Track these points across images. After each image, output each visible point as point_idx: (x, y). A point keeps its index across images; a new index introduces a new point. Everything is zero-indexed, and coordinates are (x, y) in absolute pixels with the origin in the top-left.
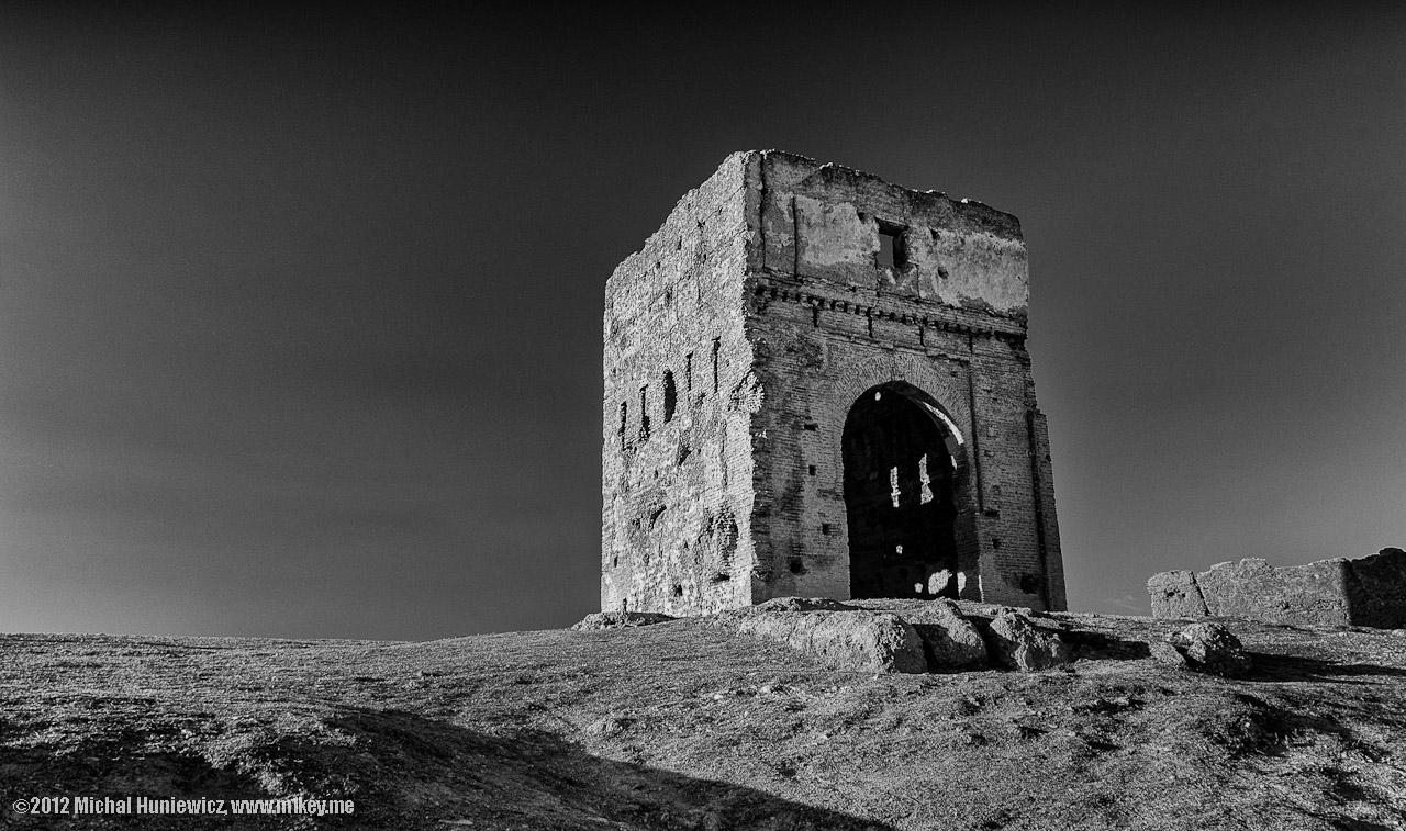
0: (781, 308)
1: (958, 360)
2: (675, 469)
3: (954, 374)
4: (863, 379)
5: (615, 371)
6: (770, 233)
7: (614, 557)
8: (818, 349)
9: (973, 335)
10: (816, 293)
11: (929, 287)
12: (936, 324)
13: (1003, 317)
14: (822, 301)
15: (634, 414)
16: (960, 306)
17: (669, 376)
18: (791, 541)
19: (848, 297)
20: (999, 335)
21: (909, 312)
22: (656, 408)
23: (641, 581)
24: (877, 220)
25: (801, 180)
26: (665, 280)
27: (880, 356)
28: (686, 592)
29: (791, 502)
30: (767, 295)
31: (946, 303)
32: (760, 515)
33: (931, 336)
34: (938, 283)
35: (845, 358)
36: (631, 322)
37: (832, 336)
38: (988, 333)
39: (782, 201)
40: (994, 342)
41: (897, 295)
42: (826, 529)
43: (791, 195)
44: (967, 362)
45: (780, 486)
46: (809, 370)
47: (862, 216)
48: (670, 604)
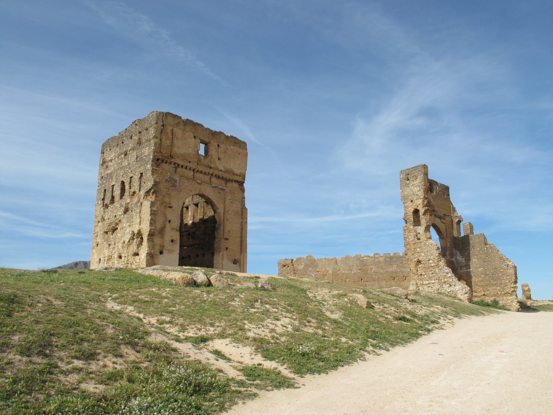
0: (164, 165)
1: (222, 188)
2: (122, 216)
3: (219, 193)
4: (189, 192)
5: (102, 177)
6: (163, 140)
7: (96, 244)
8: (176, 181)
9: (227, 181)
10: (177, 162)
11: (215, 163)
12: (216, 176)
13: (237, 175)
14: (178, 165)
15: (109, 195)
16: (224, 170)
17: (123, 183)
18: (161, 244)
19: (188, 164)
20: (236, 181)
21: (207, 171)
22: (117, 192)
23: (107, 253)
24: (200, 139)
25: (176, 123)
26: (125, 149)
27: (197, 186)
28: (123, 258)
29: (162, 231)
30: (160, 161)
31: (220, 169)
32: (151, 235)
33: (213, 179)
34: (218, 162)
35: (185, 185)
36: (111, 161)
37: (181, 177)
38: (232, 180)
39: (169, 129)
40: (234, 183)
41: (204, 165)
42: (172, 241)
43: (172, 128)
44: (224, 190)
45: (159, 226)
46: (172, 188)
47: (195, 137)
48: (117, 262)
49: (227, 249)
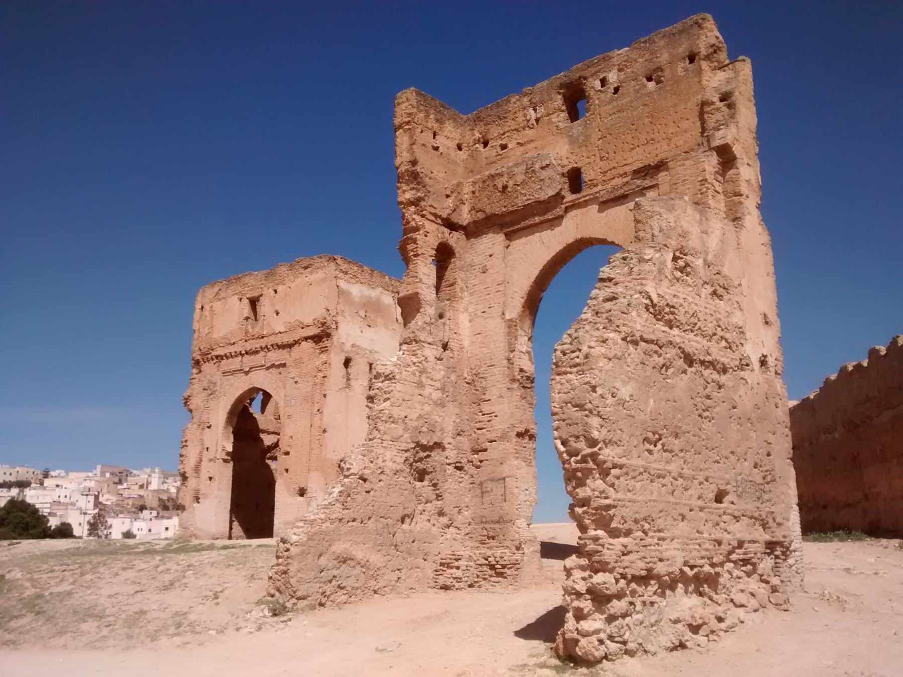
3: (280, 373)
19: (232, 349)
20: (306, 339)
40: (304, 343)
46: (211, 396)
49: (287, 470)
